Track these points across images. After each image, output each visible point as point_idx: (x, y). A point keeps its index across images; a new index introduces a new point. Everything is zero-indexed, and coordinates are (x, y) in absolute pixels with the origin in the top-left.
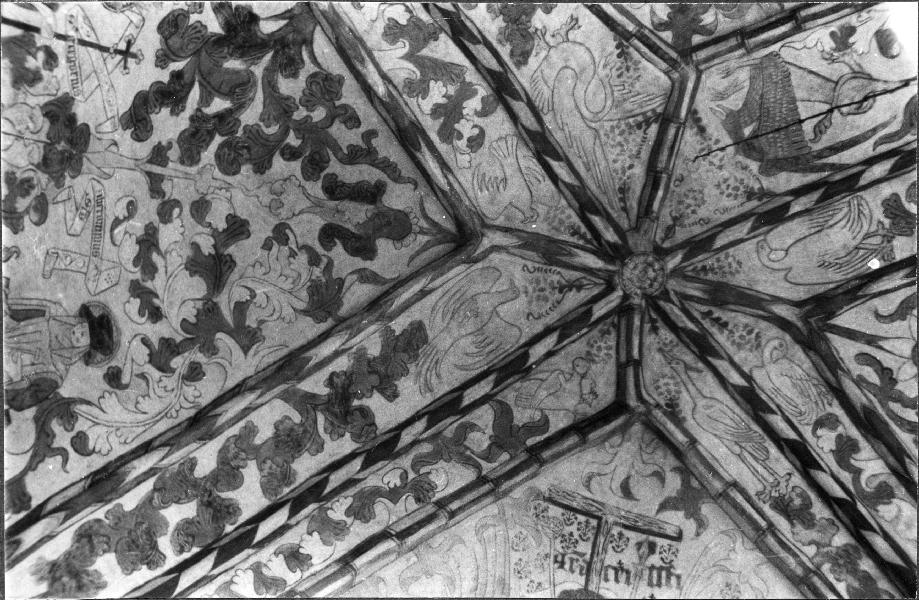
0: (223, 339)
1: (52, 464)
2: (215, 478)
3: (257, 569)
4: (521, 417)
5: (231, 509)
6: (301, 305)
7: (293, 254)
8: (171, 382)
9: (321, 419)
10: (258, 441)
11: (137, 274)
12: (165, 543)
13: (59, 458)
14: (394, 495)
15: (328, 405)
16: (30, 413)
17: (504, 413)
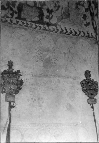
1: (85, 5)
13: (84, 4)
16: (79, 6)
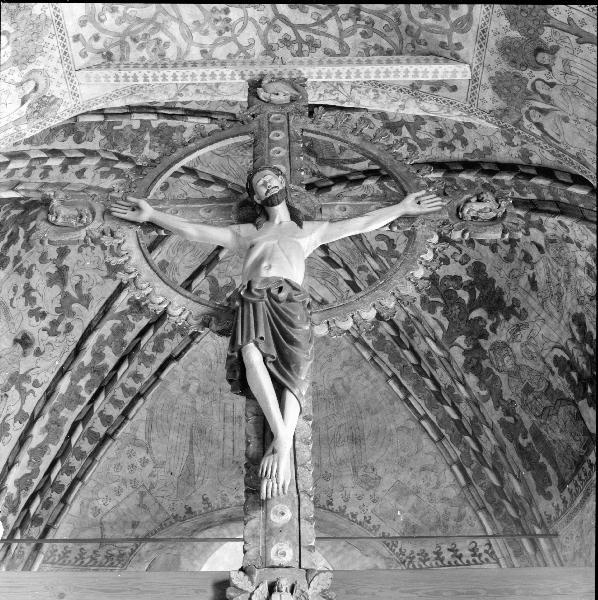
0: (75, 306)
2: (93, 361)
3: (123, 386)
4: (222, 282)
5: (105, 367)
6: (105, 274)
7: (93, 248)
8: (61, 338)
9: (130, 317)
10: (105, 338)
11: (29, 307)
12: (83, 393)
14: (171, 335)
15: (131, 311)
16: (13, 388)
17: (214, 281)
